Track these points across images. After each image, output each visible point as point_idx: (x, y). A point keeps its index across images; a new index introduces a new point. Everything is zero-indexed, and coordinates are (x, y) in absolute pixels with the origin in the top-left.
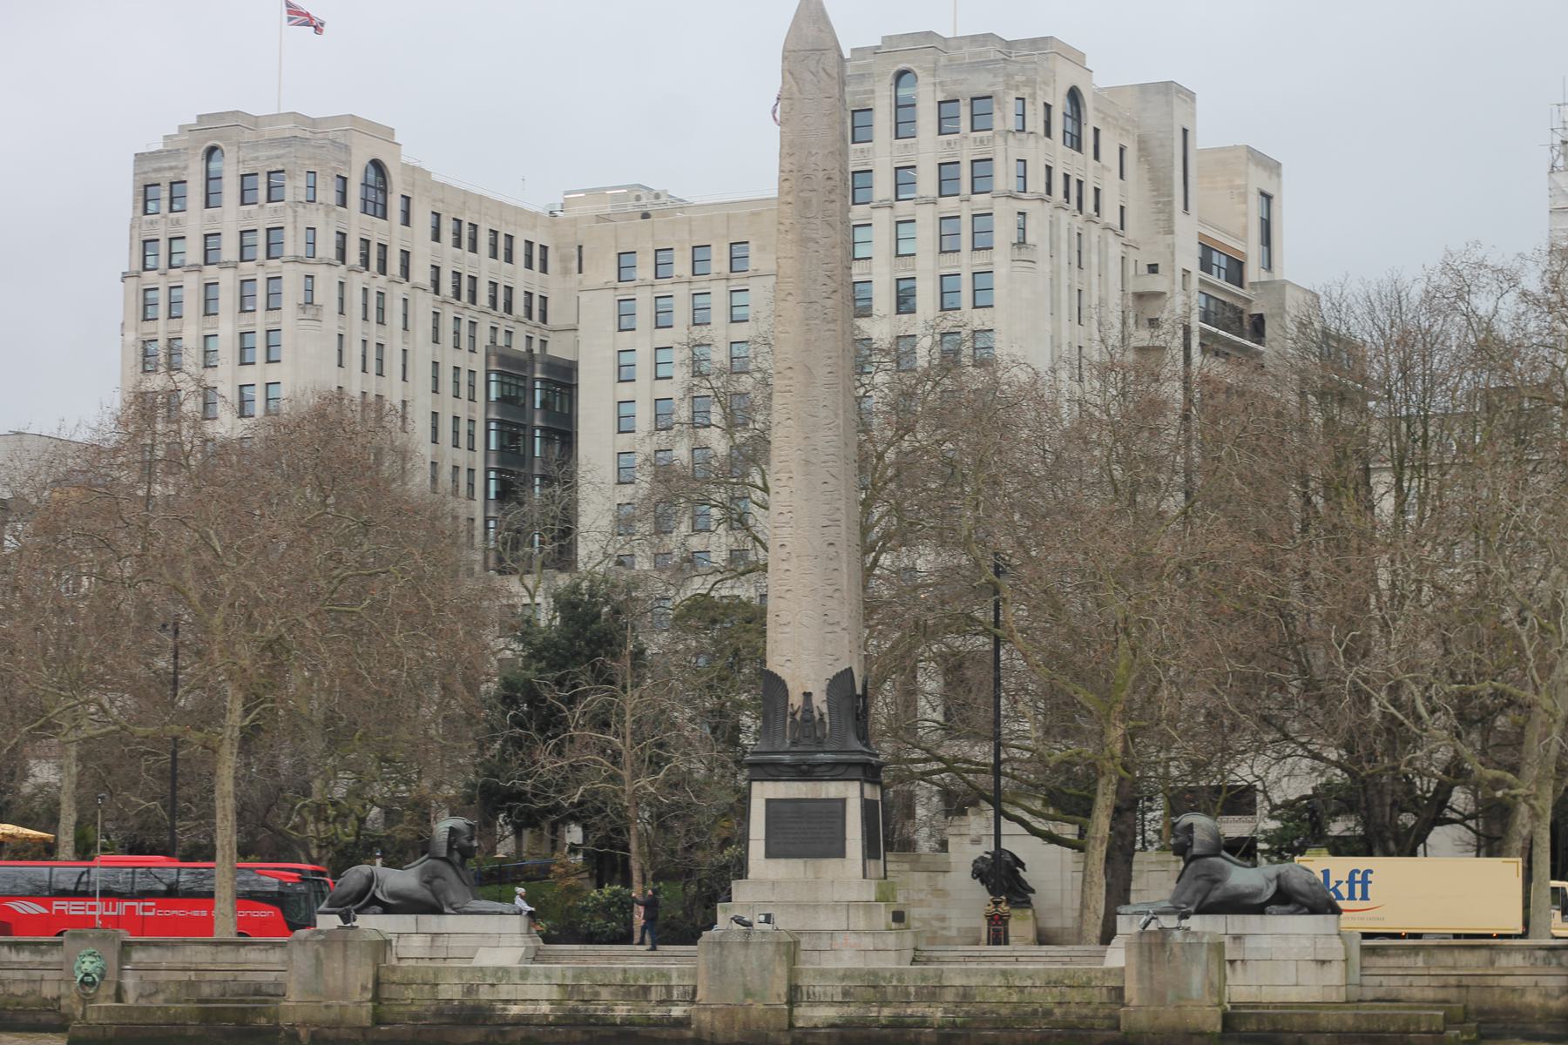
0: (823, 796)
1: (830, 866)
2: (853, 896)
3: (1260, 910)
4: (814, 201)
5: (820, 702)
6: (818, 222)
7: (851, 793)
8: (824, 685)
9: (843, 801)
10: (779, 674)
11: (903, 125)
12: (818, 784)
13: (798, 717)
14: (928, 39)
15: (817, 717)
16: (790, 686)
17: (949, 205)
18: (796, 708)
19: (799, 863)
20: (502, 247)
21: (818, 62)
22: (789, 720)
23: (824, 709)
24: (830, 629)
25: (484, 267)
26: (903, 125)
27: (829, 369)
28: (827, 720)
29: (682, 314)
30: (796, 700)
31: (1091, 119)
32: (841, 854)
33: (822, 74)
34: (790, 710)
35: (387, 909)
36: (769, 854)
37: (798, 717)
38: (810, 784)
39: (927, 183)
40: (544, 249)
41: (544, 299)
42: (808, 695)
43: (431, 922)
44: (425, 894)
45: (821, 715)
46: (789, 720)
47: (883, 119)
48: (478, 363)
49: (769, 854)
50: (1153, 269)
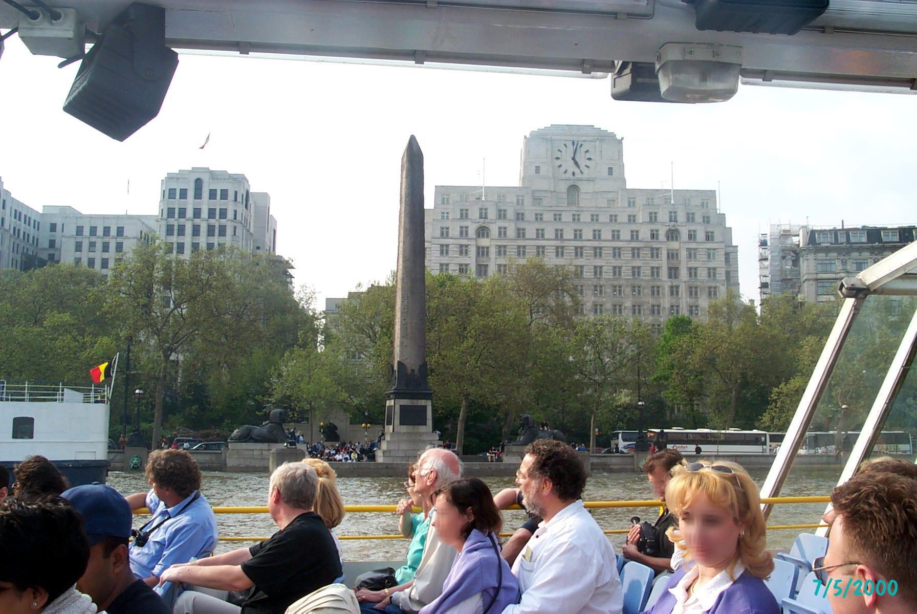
1: (422, 429)
7: (428, 404)
9: (425, 407)
11: (198, 195)
14: (207, 170)
17: (212, 221)
20: (27, 220)
25: (23, 227)
26: (198, 195)
29: (112, 246)
31: (251, 202)
32: (425, 424)
35: (256, 441)
36: (401, 423)
39: (205, 214)
40: (39, 223)
41: (37, 239)
47: (191, 194)
48: (19, 257)
49: (401, 423)
50: (258, 248)
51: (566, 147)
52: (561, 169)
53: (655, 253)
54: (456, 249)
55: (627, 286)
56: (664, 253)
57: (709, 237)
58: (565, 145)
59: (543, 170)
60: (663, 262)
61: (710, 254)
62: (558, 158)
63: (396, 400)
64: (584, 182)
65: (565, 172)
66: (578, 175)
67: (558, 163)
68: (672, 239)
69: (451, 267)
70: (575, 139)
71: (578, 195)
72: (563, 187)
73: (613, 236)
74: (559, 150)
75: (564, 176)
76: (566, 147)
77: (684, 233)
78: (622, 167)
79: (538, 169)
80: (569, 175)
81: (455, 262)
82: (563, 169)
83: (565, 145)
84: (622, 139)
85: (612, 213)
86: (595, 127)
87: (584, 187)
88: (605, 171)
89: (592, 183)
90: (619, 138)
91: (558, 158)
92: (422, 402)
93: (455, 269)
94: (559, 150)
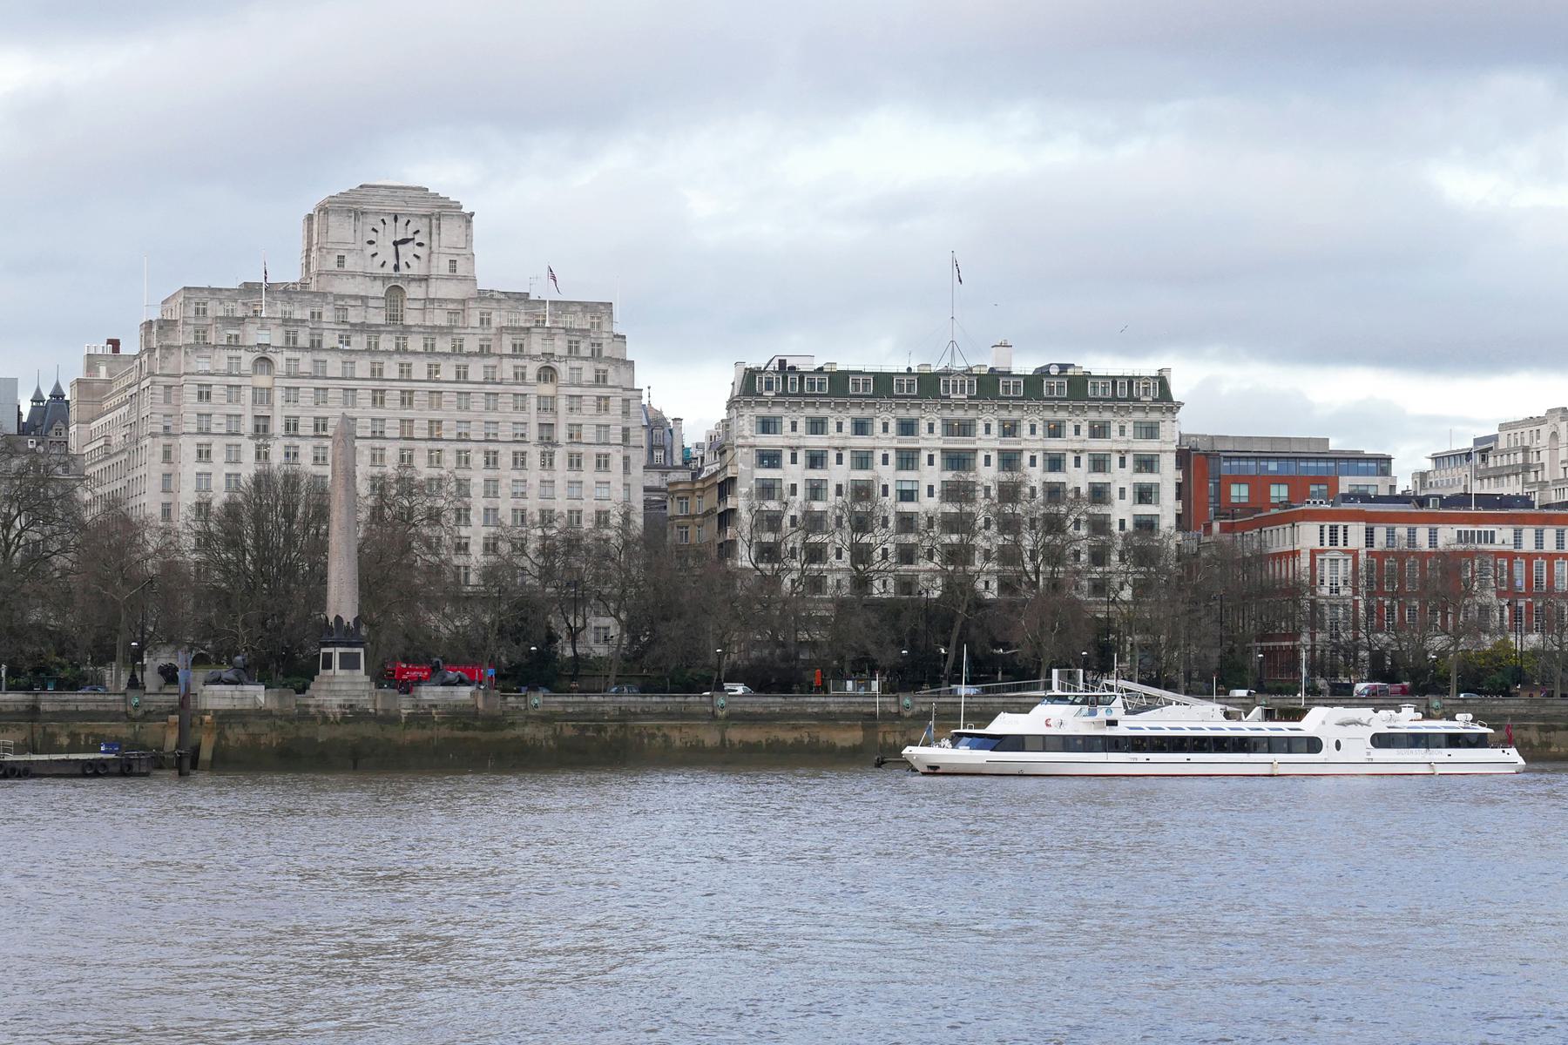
1: (356, 671)
2: (361, 680)
3: (455, 685)
5: (352, 624)
7: (362, 651)
19: (347, 671)
30: (345, 624)
35: (226, 684)
43: (240, 687)
44: (236, 679)
51: (385, 223)
52: (376, 258)
53: (520, 400)
54: (222, 392)
55: (477, 452)
56: (533, 402)
57: (600, 379)
58: (383, 220)
59: (349, 264)
60: (533, 418)
61: (602, 404)
62: (371, 242)
64: (414, 284)
65: (383, 265)
66: (404, 270)
67: (371, 249)
68: (546, 381)
69: (215, 419)
70: (398, 210)
71: (402, 301)
72: (378, 289)
73: (458, 374)
74: (374, 230)
75: (381, 271)
76: (385, 223)
77: (563, 369)
78: (471, 257)
79: (341, 259)
80: (389, 269)
81: (222, 411)
82: (378, 260)
83: (383, 220)
84: (472, 215)
85: (455, 336)
86: (430, 191)
87: (414, 291)
88: (442, 266)
89: (423, 284)
90: (465, 210)
91: (371, 242)
92: (356, 650)
93: (220, 421)
94: (374, 230)
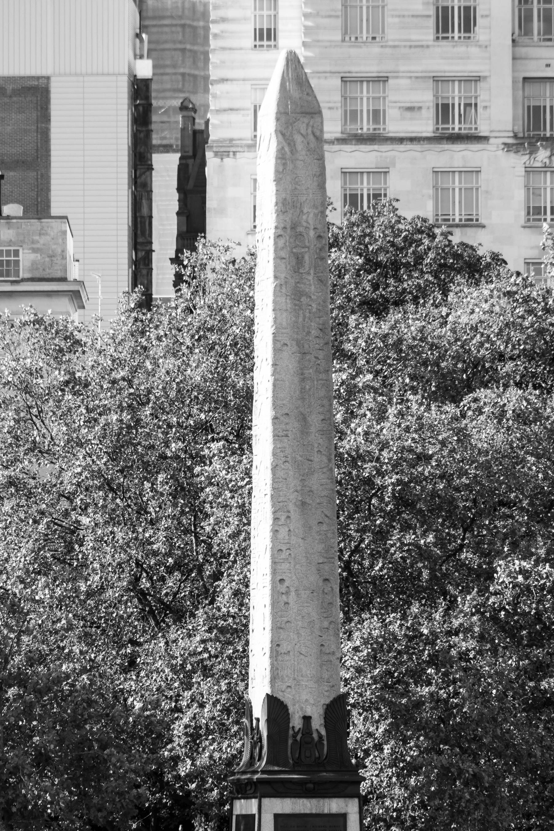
0: (326, 811)
4: (307, 257)
5: (317, 724)
6: (310, 278)
8: (321, 711)
10: (282, 699)
12: (321, 801)
13: (298, 738)
15: (315, 735)
16: (291, 710)
18: (296, 730)
21: (308, 125)
22: (290, 742)
23: (323, 732)
24: (326, 658)
27: (322, 417)
28: (325, 738)
30: (296, 723)
33: (311, 137)
34: (291, 732)
37: (298, 738)
38: (314, 801)
42: (307, 719)
45: (320, 737)
46: (290, 742)
63: (266, 802)
